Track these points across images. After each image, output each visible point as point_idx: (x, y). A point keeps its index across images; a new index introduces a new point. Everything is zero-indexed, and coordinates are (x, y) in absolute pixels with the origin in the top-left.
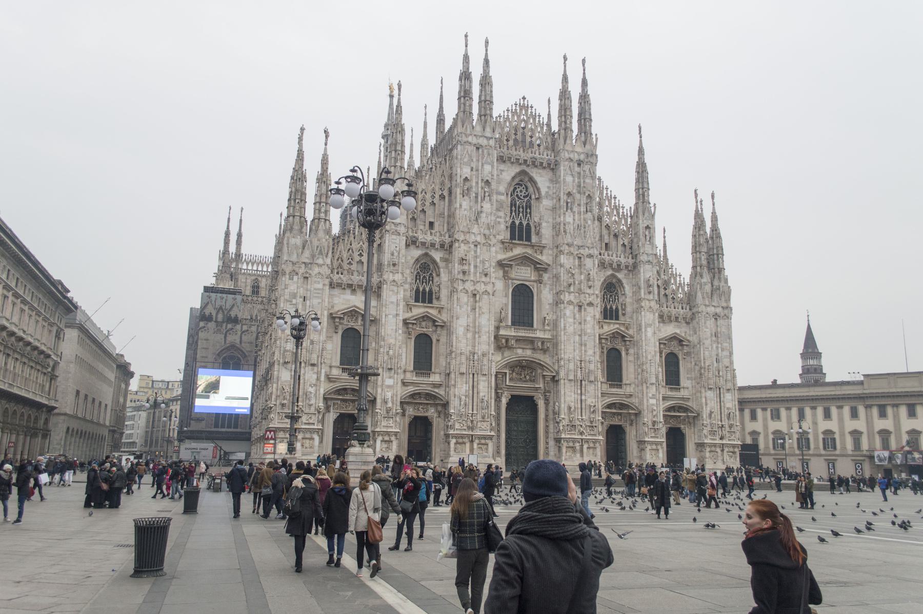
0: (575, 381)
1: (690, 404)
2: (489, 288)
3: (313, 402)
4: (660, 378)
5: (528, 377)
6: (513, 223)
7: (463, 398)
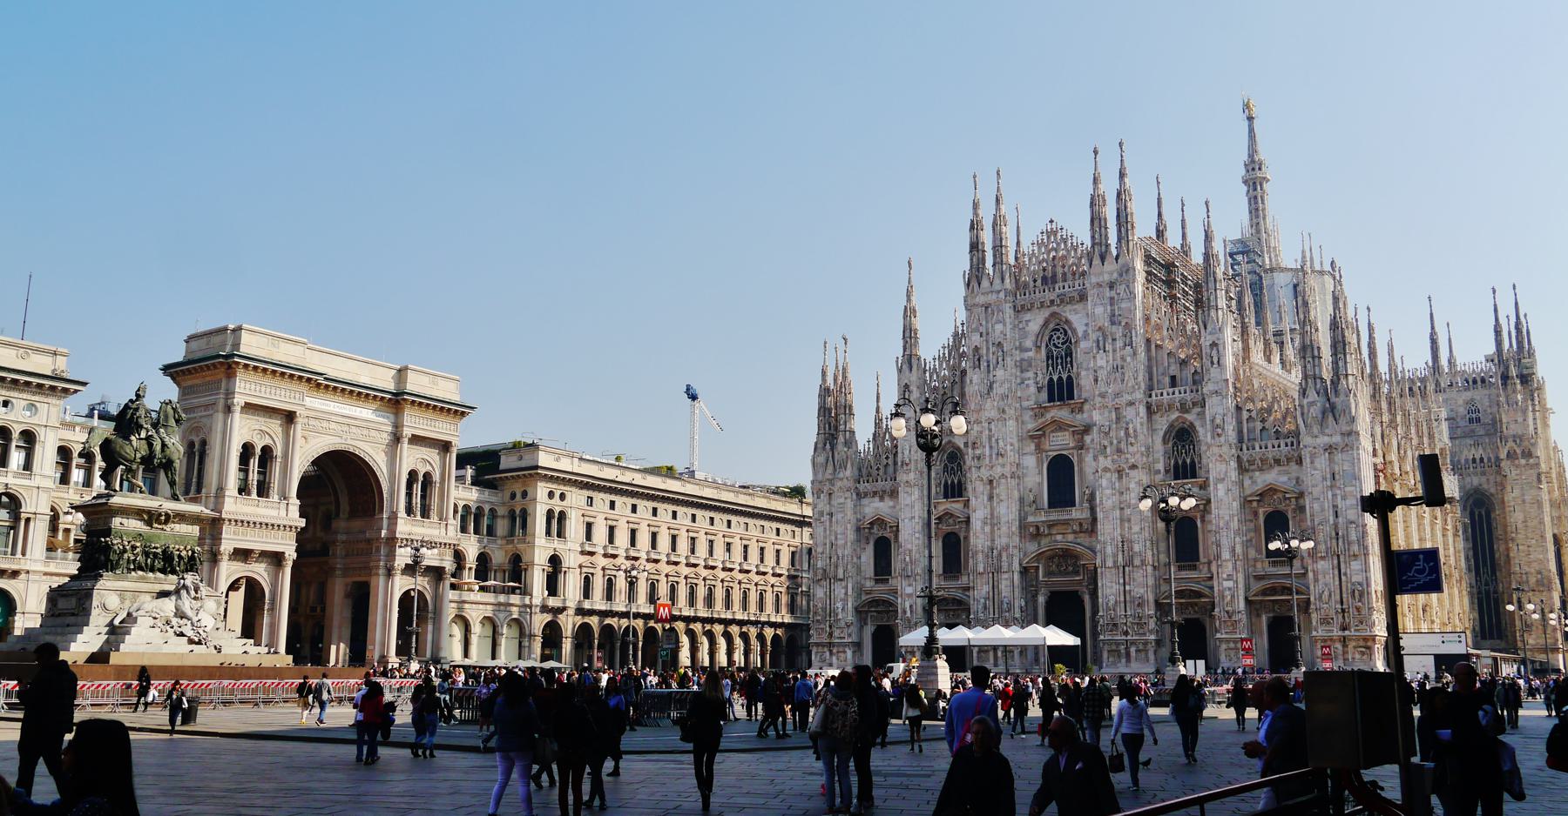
0: (1116, 566)
1: (1295, 583)
4: (1239, 549)
6: (1051, 380)
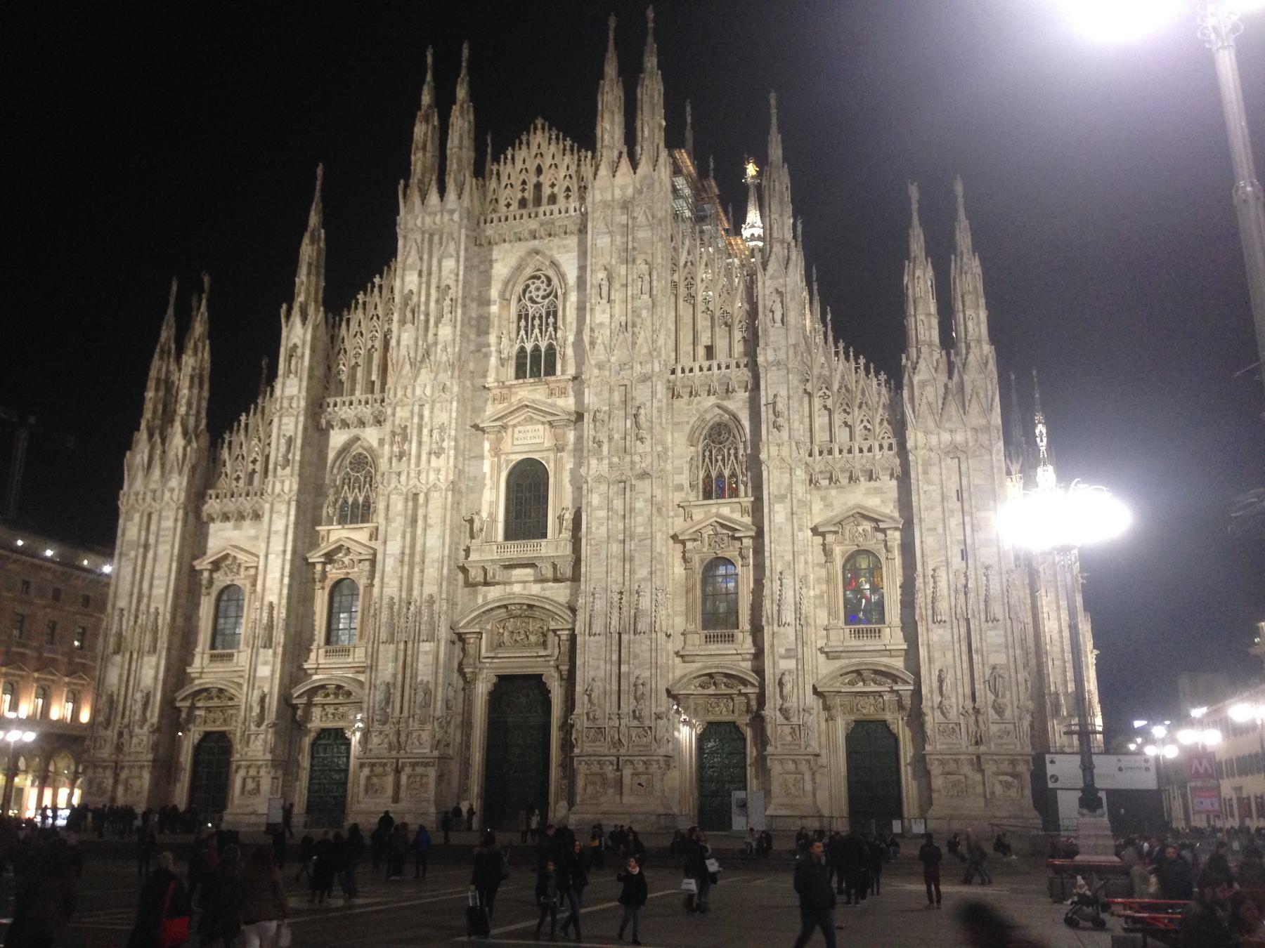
5: (533, 638)
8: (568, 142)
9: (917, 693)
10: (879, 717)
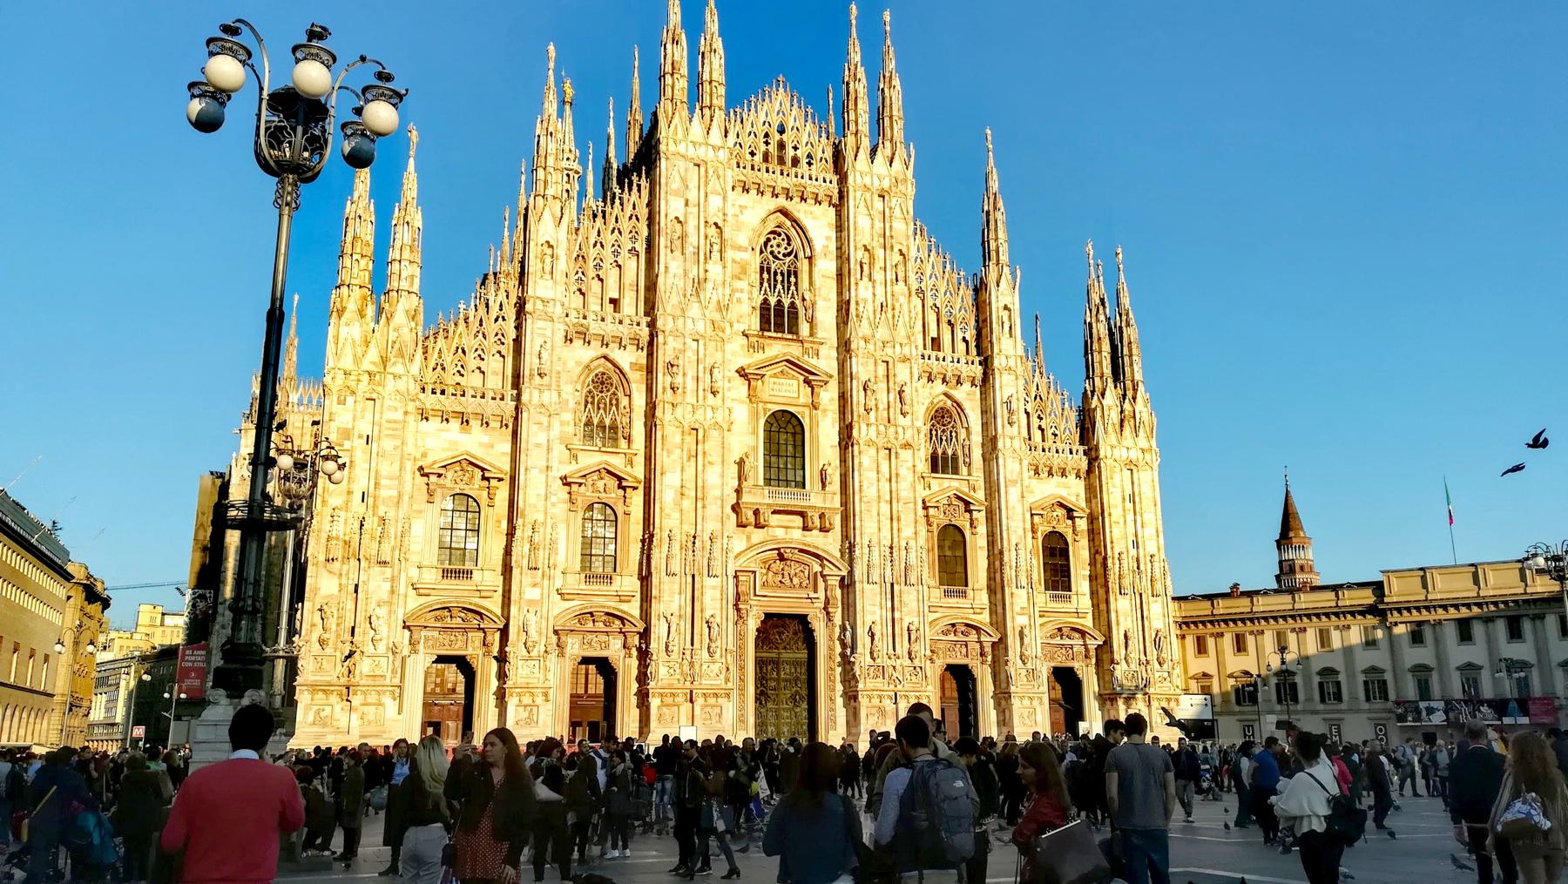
2: (720, 417)
3: (383, 631)
5: (796, 581)
7: (674, 620)
8: (810, 110)
9: (1107, 645)
10: (1069, 664)
